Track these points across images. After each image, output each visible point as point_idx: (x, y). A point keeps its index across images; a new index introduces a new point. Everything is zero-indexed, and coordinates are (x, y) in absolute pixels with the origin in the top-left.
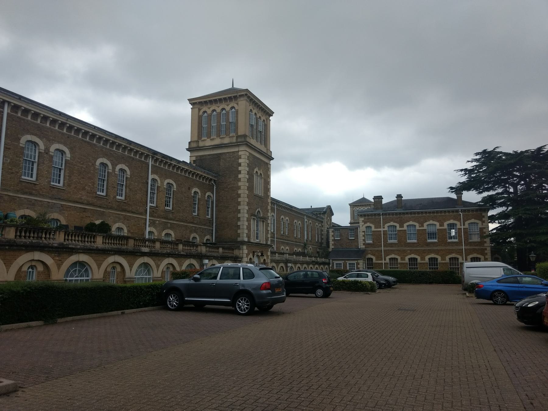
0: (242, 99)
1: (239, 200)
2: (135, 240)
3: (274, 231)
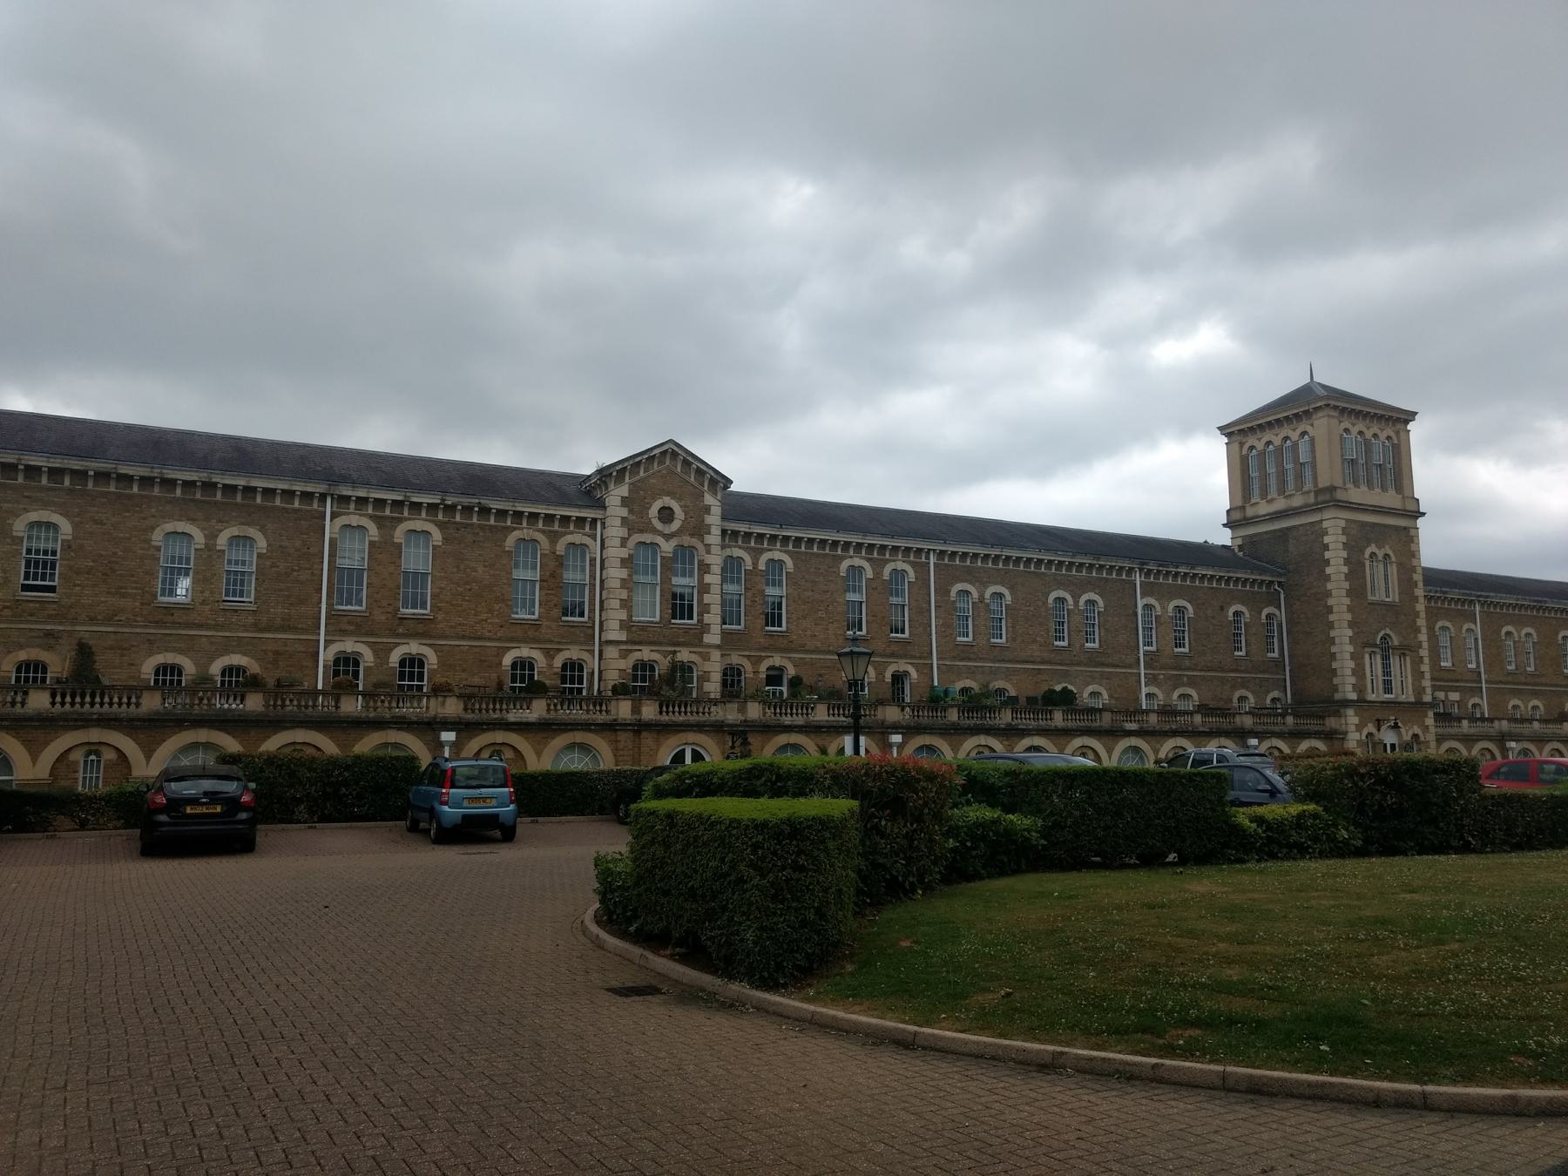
0: (1320, 414)
1: (1332, 618)
2: (1112, 712)
3: (1478, 666)
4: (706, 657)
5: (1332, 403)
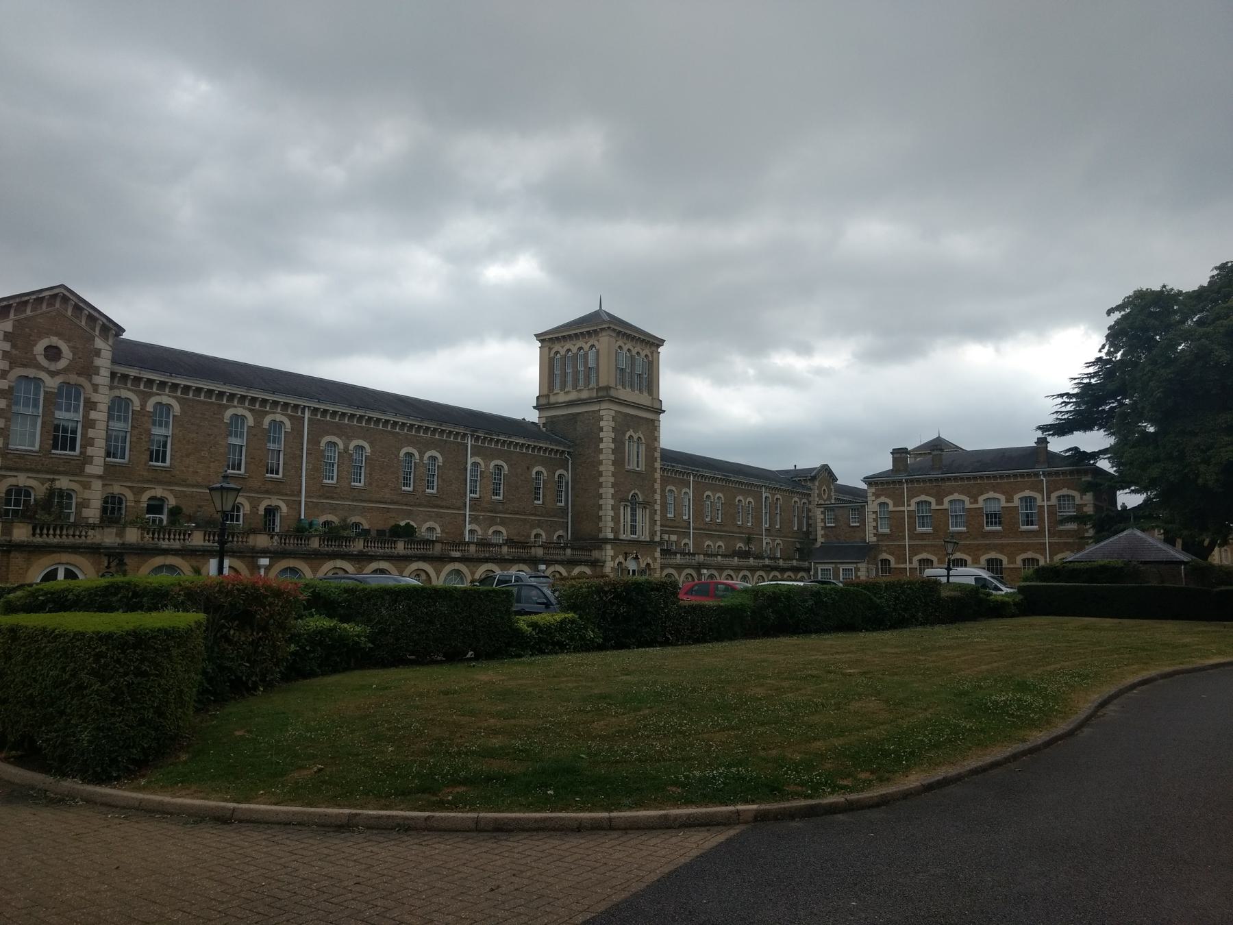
0: (604, 334)
1: (601, 480)
2: (442, 543)
3: (689, 518)
4: (86, 486)
5: (612, 326)
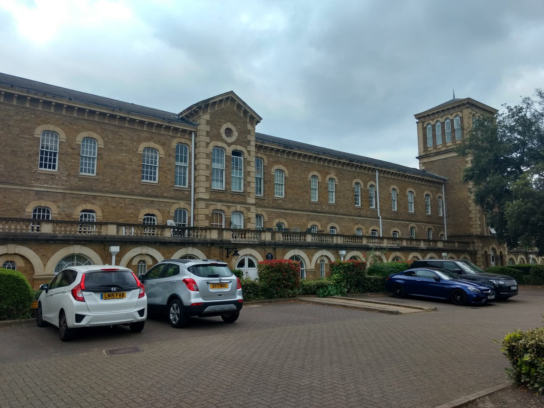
4: (249, 210)
